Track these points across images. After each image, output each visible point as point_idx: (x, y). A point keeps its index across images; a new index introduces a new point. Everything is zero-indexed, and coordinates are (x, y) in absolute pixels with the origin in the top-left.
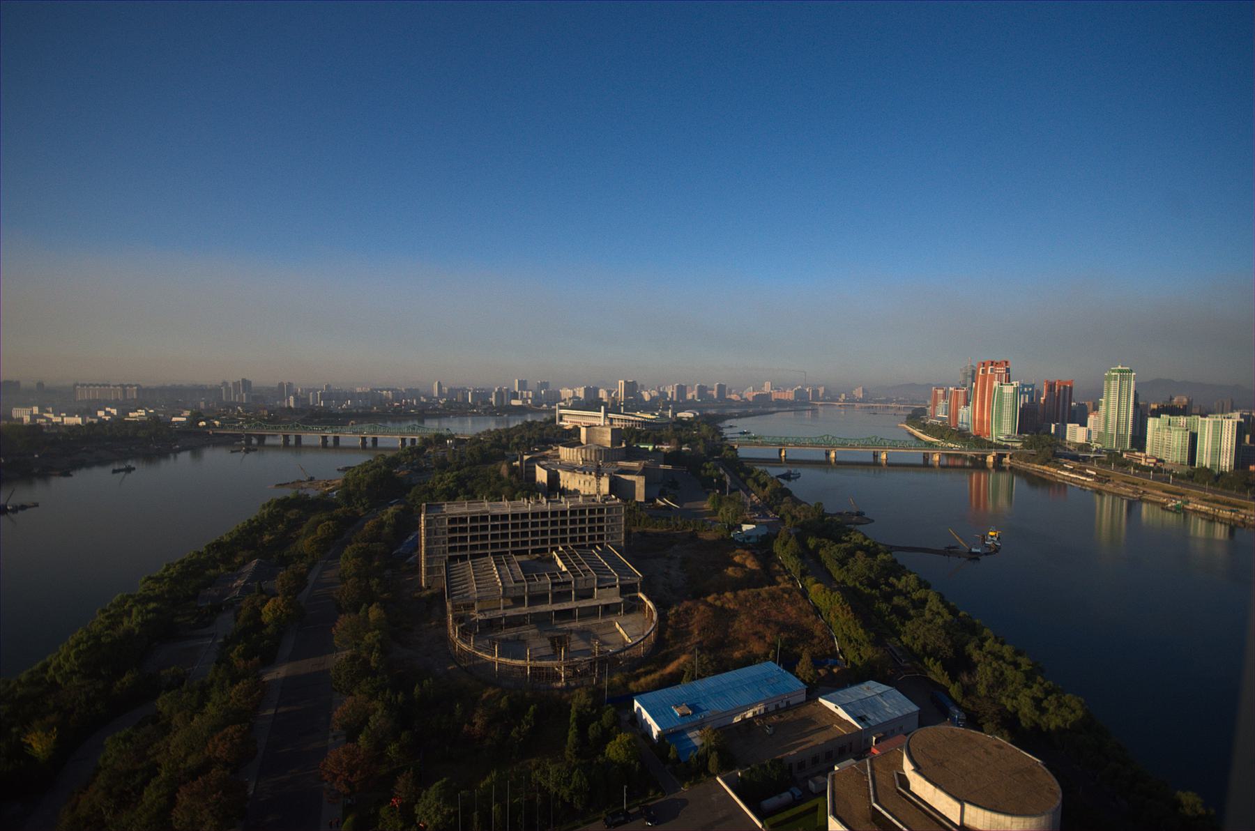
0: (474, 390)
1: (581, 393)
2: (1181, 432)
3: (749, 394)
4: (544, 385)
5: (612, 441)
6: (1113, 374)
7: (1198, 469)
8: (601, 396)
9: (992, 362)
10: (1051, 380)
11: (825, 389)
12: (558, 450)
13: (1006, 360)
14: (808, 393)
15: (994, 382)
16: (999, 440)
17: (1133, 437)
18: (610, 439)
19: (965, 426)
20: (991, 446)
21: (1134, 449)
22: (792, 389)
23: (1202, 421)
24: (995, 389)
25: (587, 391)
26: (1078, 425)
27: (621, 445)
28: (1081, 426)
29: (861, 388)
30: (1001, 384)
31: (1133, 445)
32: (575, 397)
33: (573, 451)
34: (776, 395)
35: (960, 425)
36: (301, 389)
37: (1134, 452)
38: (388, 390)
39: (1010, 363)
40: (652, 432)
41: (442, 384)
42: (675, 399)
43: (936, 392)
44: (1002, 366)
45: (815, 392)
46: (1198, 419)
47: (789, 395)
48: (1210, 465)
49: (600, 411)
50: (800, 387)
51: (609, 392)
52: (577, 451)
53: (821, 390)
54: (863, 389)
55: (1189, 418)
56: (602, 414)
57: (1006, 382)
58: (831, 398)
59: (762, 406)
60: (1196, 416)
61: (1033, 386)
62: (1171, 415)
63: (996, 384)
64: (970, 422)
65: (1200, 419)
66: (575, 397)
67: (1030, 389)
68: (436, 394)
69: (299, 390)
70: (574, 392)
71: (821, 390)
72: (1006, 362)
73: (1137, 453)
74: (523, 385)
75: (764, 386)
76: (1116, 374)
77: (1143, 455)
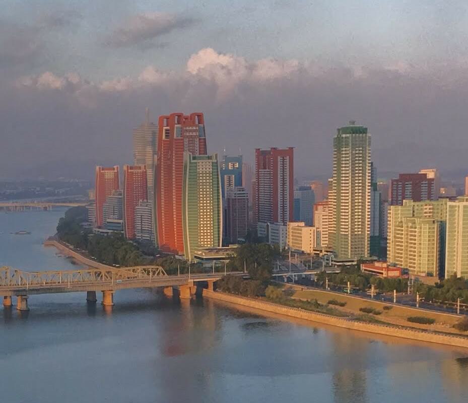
2: (427, 226)
6: (344, 136)
7: (448, 279)
9: (179, 116)
10: (265, 147)
13: (199, 111)
15: (184, 153)
16: (196, 257)
17: (372, 238)
19: (146, 236)
20: (185, 268)
21: (375, 258)
23: (451, 207)
24: (186, 167)
26: (303, 224)
28: (307, 225)
30: (194, 158)
31: (371, 254)
35: (139, 236)
37: (372, 261)
39: (205, 118)
43: (102, 175)
44: (193, 124)
46: (446, 204)
48: (462, 273)
55: (435, 203)
57: (200, 154)
60: (444, 200)
61: (239, 160)
62: (414, 201)
63: (187, 156)
64: (154, 230)
65: (449, 203)
67: (237, 165)
72: (200, 116)
73: (377, 264)
76: (348, 135)
77: (385, 265)
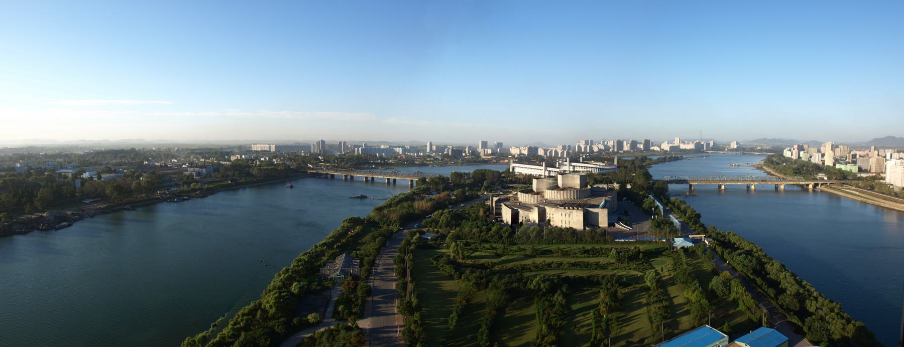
0: (452, 147)
1: (525, 152)
3: (666, 147)
4: (499, 145)
5: (580, 184)
8: (539, 154)
11: (714, 142)
12: (517, 194)
14: (703, 145)
18: (579, 183)
22: (693, 143)
25: (530, 149)
27: (587, 186)
29: (735, 142)
32: (521, 154)
33: (554, 193)
34: (682, 147)
36: (351, 146)
38: (399, 147)
40: (603, 177)
41: (432, 144)
42: (616, 150)
45: (708, 144)
47: (691, 146)
49: (542, 166)
50: (698, 141)
51: (546, 151)
52: (557, 193)
53: (712, 144)
54: (737, 142)
56: (543, 168)
58: (717, 148)
59: (675, 155)
66: (521, 154)
68: (428, 150)
69: (349, 146)
70: (520, 150)
71: (712, 144)
74: (485, 145)
75: (674, 140)
